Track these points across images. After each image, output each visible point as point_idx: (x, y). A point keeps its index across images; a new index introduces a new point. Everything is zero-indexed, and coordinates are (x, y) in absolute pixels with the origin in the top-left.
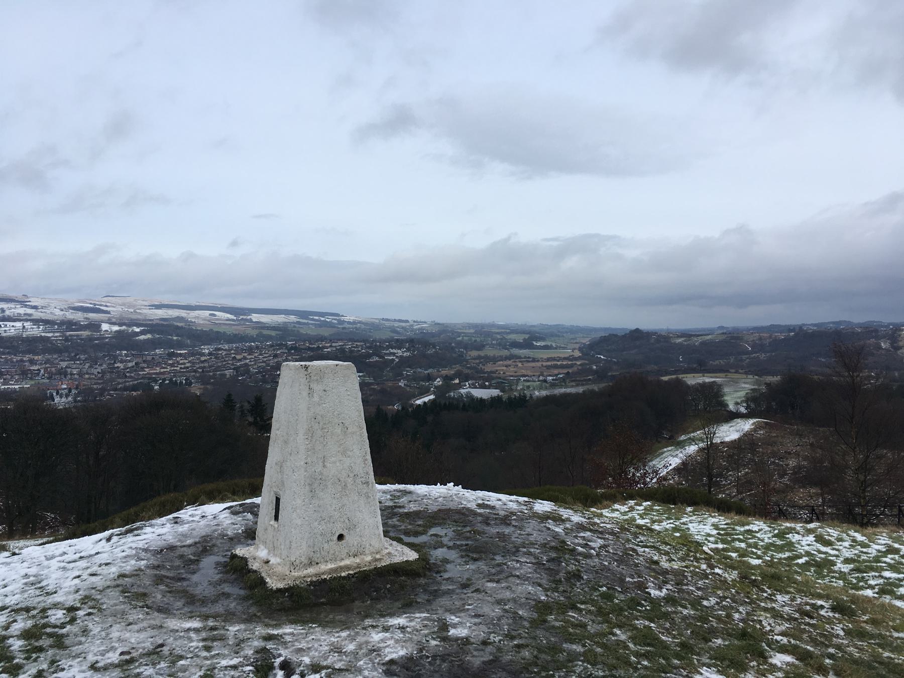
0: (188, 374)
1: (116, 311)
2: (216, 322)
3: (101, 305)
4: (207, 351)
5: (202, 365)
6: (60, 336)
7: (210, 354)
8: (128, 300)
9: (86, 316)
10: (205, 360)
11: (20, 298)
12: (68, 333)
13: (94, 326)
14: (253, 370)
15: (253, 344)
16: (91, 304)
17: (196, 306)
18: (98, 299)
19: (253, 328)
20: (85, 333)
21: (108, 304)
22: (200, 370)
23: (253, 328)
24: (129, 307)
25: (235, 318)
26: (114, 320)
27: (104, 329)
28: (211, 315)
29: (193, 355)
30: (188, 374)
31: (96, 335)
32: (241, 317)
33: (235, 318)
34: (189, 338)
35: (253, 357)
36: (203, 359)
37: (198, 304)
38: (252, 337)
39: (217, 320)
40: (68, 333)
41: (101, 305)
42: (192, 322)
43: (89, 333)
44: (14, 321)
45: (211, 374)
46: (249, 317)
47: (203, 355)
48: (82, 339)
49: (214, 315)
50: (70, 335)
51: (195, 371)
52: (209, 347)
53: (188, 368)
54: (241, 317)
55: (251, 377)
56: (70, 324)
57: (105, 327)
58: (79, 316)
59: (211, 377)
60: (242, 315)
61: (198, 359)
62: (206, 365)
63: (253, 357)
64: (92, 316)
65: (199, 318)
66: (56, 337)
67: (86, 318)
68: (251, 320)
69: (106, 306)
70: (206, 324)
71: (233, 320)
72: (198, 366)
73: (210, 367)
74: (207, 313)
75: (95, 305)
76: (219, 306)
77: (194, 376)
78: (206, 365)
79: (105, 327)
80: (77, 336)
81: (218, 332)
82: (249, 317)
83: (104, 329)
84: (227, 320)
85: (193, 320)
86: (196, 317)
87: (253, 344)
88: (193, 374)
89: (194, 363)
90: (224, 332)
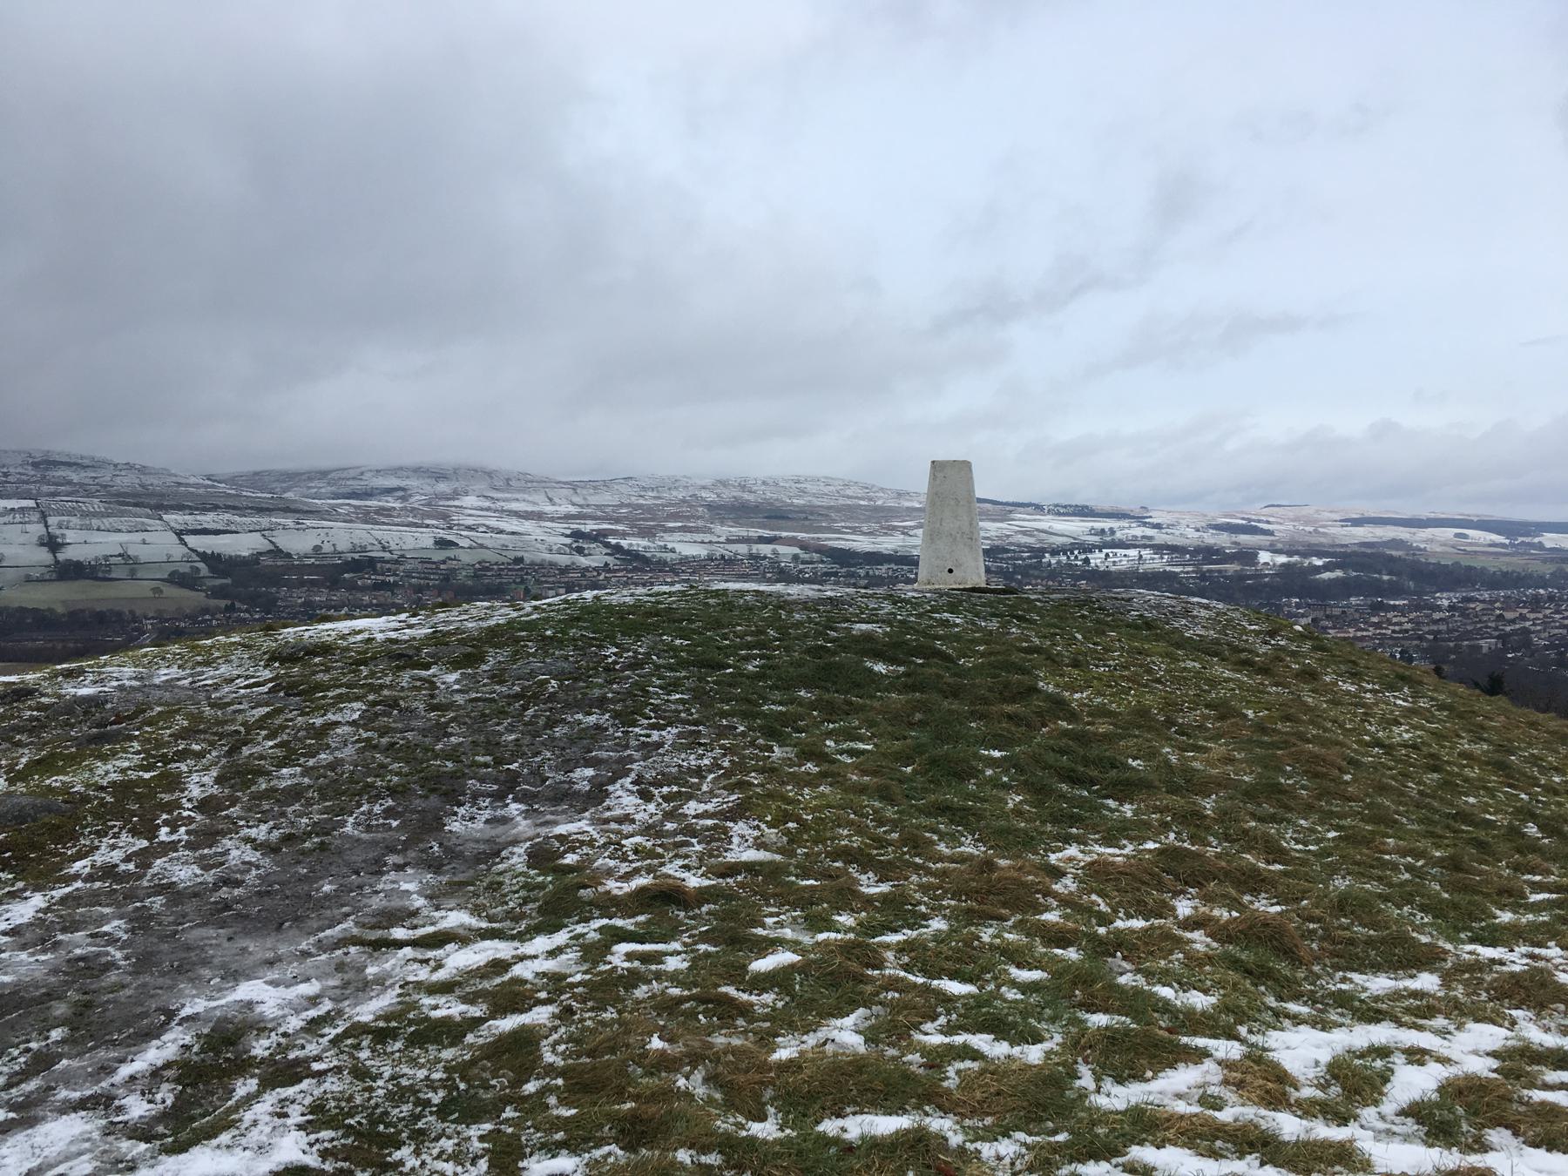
0: (1407, 643)
1: (1283, 529)
2: (1468, 549)
3: (1259, 521)
4: (1446, 603)
5: (1435, 628)
6: (1193, 572)
7: (1452, 608)
8: (1305, 511)
9: (1234, 539)
10: (1441, 619)
11: (1138, 512)
12: (1206, 567)
13: (1248, 556)
14: (1539, 641)
15: (1542, 591)
16: (1243, 519)
17: (1429, 520)
18: (1255, 511)
19: (1545, 561)
20: (1232, 568)
21: (1271, 519)
22: (1431, 637)
23: (1545, 561)
24: (1306, 523)
25: (1507, 541)
26: (1280, 546)
27: (1262, 561)
28: (1457, 535)
29: (1418, 608)
30: (1407, 643)
31: (1249, 570)
32: (1520, 539)
33: (1507, 541)
34: (1412, 579)
35: (1540, 616)
36: (1437, 616)
37: (1432, 515)
38: (1542, 577)
39: (1471, 544)
40: (1206, 567)
41: (1259, 521)
42: (1420, 550)
43: (1238, 568)
44: (1128, 547)
45: (1452, 644)
46: (1536, 540)
47: (1439, 608)
48: (1226, 578)
49: (1465, 536)
50: (1210, 571)
51: (1420, 638)
52: (1452, 594)
53: (1407, 631)
54: (1520, 539)
55: (1532, 655)
56: (1209, 553)
57: (1264, 557)
58: (1223, 540)
59: (1451, 651)
60: (1522, 536)
61: (1427, 616)
62: (1443, 627)
63: (1540, 616)
64: (1244, 538)
65: (1435, 542)
66: (1187, 573)
67: (1235, 543)
68: (1540, 546)
69: (1268, 522)
70: (1447, 553)
71: (1503, 545)
72: (1426, 629)
73: (1449, 631)
74: (1449, 532)
75: (1249, 520)
76: (1475, 519)
77: (1417, 646)
78: (1443, 627)
79: (1264, 557)
80: (1219, 571)
81: (1470, 568)
82: (1536, 540)
83: (1262, 561)
84: (1490, 545)
85: (1422, 546)
86: (1426, 541)
87: (1542, 591)
88: (1415, 642)
89: (1418, 623)
90: (1483, 569)
